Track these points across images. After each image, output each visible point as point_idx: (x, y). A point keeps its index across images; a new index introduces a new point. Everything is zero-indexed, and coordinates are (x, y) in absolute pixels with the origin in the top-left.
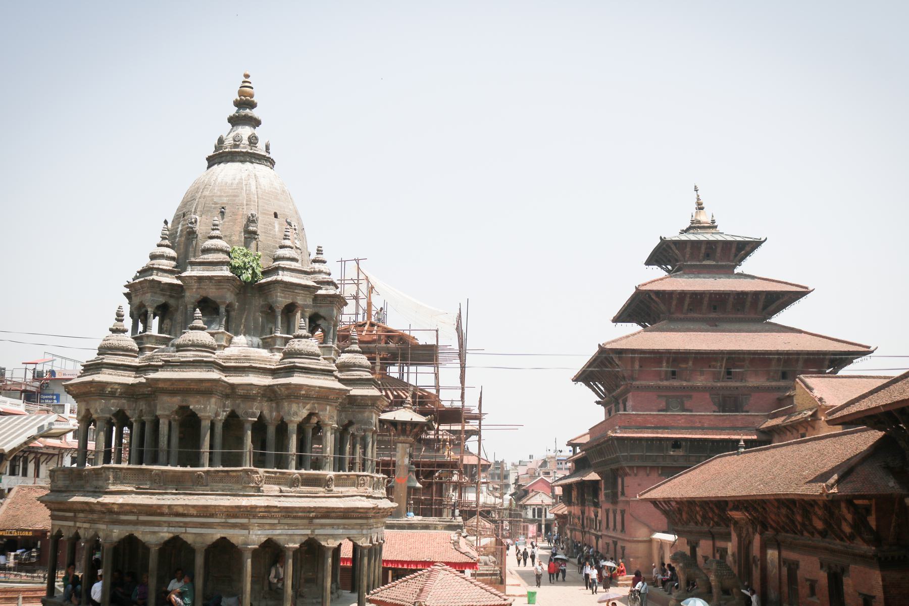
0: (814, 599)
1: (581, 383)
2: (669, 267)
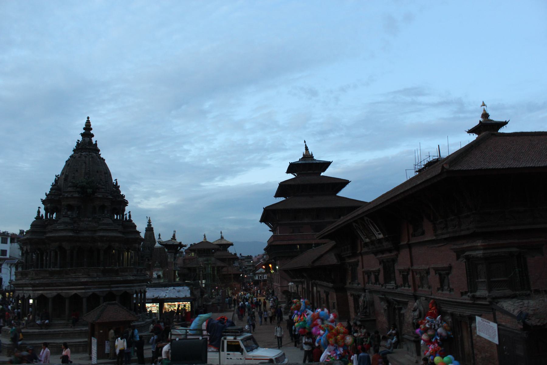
0: (324, 305)
1: (263, 223)
2: (295, 174)
